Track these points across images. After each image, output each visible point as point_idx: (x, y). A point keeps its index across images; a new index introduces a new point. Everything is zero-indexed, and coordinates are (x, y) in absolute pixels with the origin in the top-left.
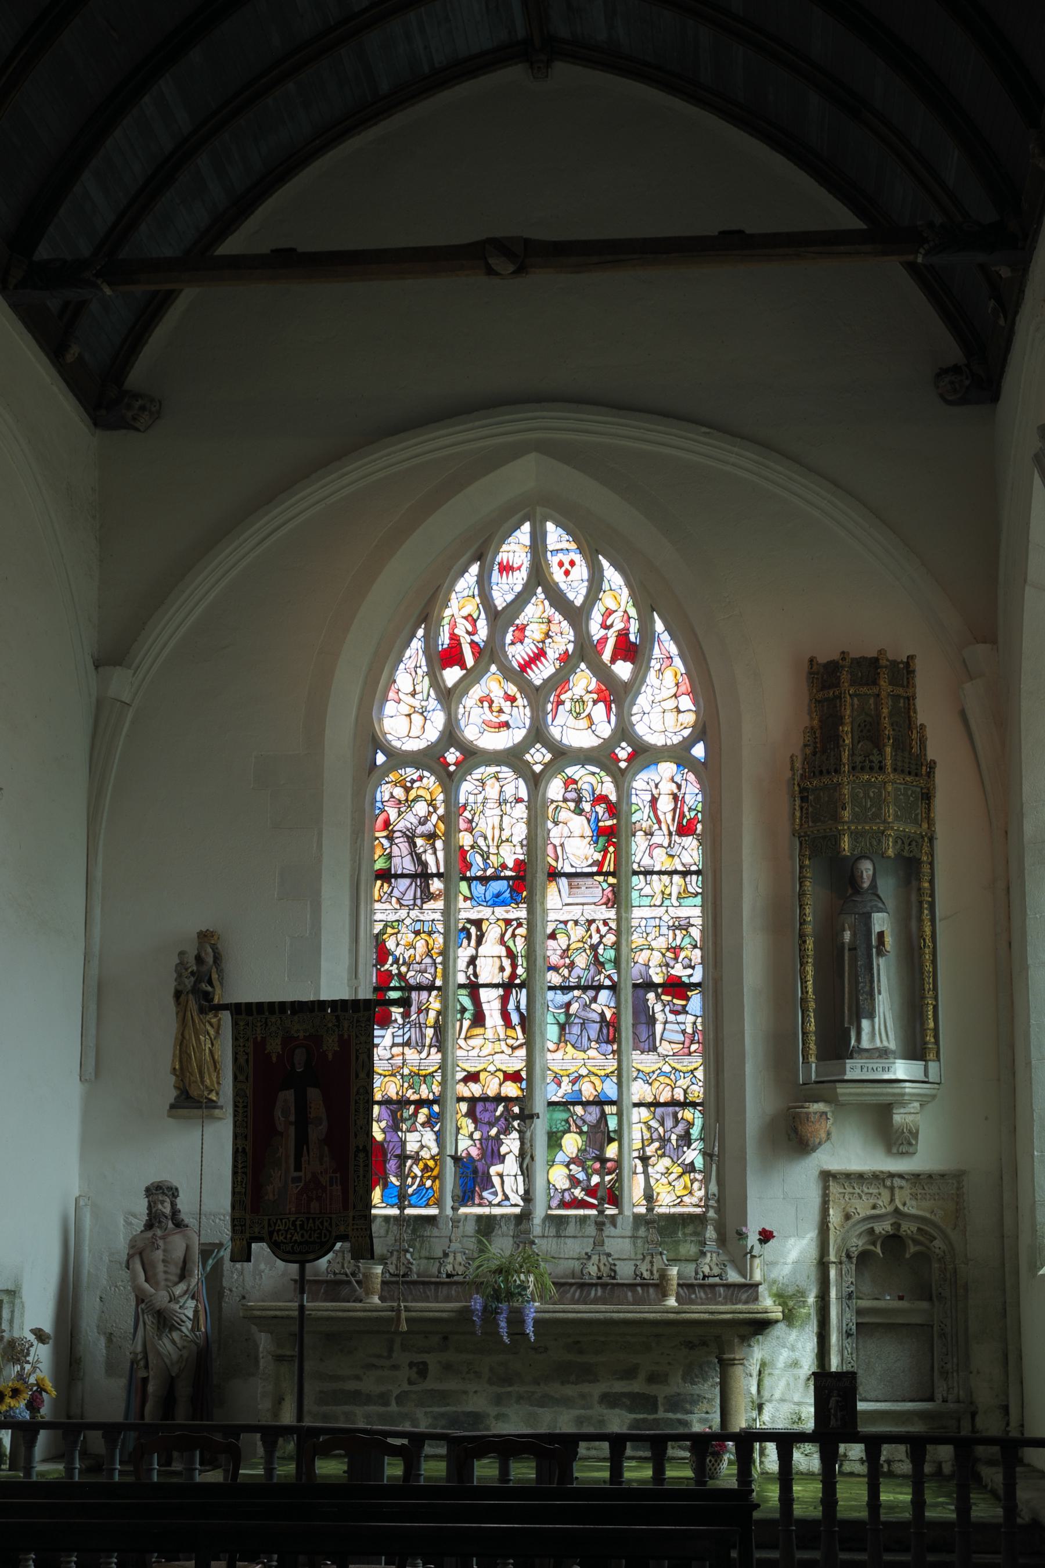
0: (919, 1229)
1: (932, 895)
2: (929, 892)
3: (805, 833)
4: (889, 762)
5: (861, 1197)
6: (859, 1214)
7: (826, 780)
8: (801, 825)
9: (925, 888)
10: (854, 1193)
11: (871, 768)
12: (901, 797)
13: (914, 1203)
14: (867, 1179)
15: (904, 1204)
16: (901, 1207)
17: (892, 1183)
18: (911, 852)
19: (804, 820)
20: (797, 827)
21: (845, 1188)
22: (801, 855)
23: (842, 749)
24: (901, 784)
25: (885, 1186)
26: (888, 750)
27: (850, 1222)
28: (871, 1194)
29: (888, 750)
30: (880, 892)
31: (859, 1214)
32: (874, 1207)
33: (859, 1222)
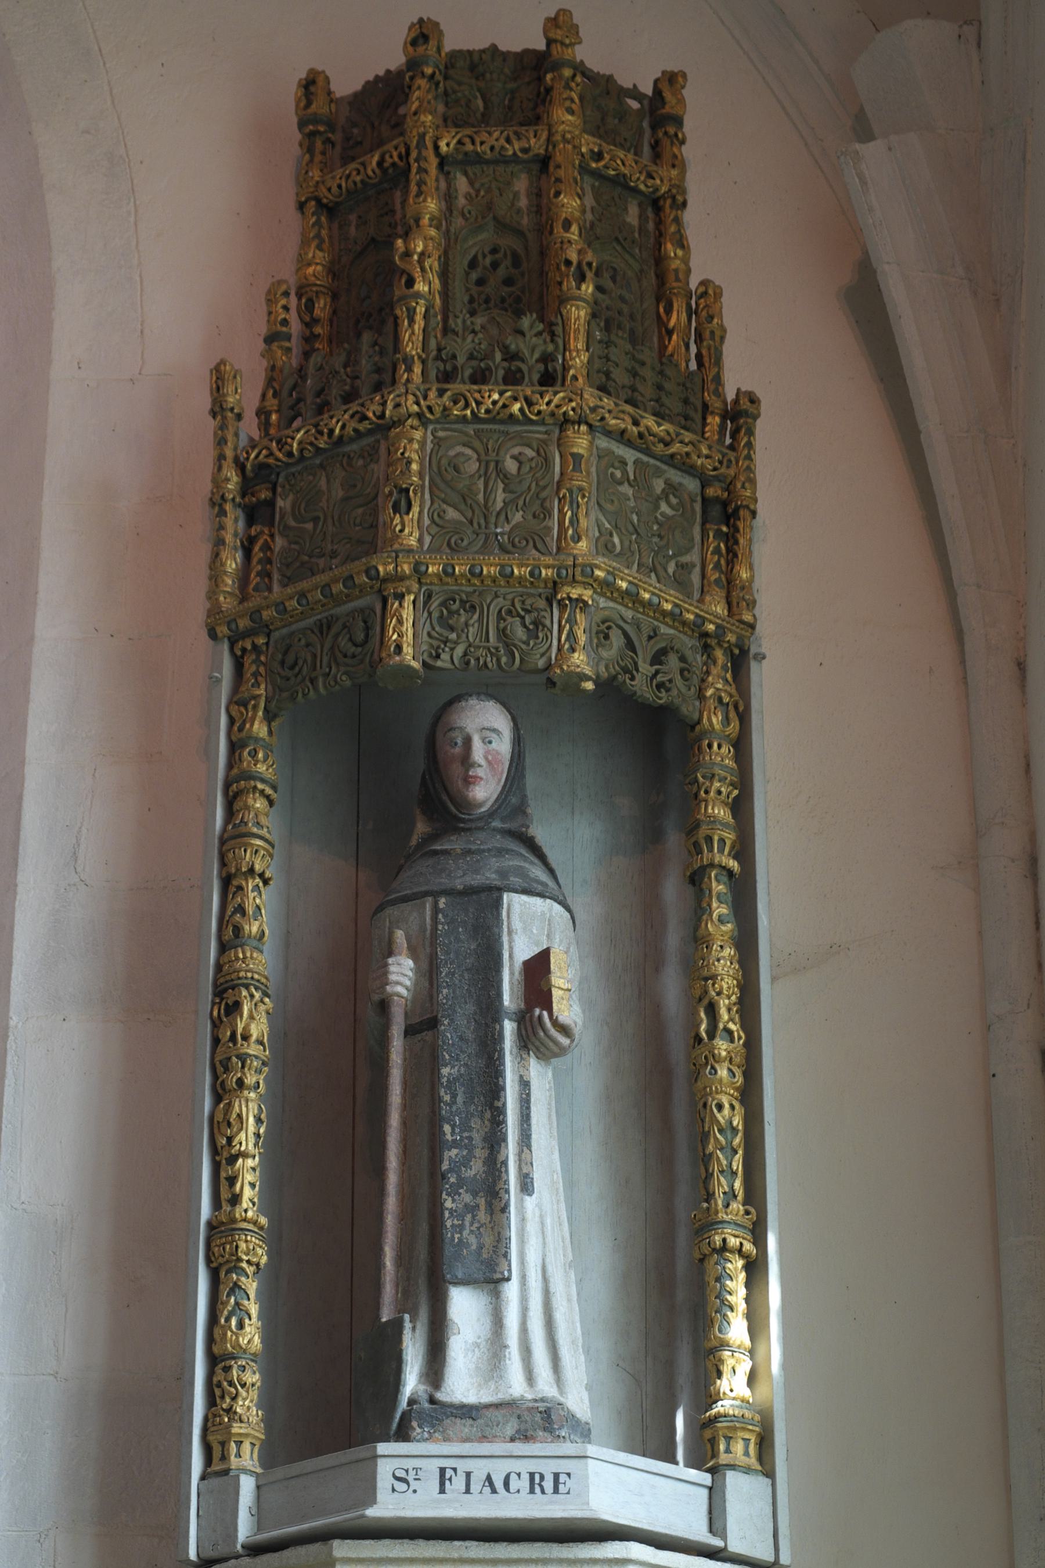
1: (744, 850)
2: (730, 836)
3: (255, 615)
4: (579, 360)
7: (339, 422)
8: (243, 599)
9: (713, 821)
11: (512, 378)
12: (626, 489)
18: (659, 686)
19: (254, 579)
20: (227, 603)
22: (239, 701)
23: (401, 312)
24: (621, 436)
26: (578, 314)
29: (578, 314)
30: (539, 832)
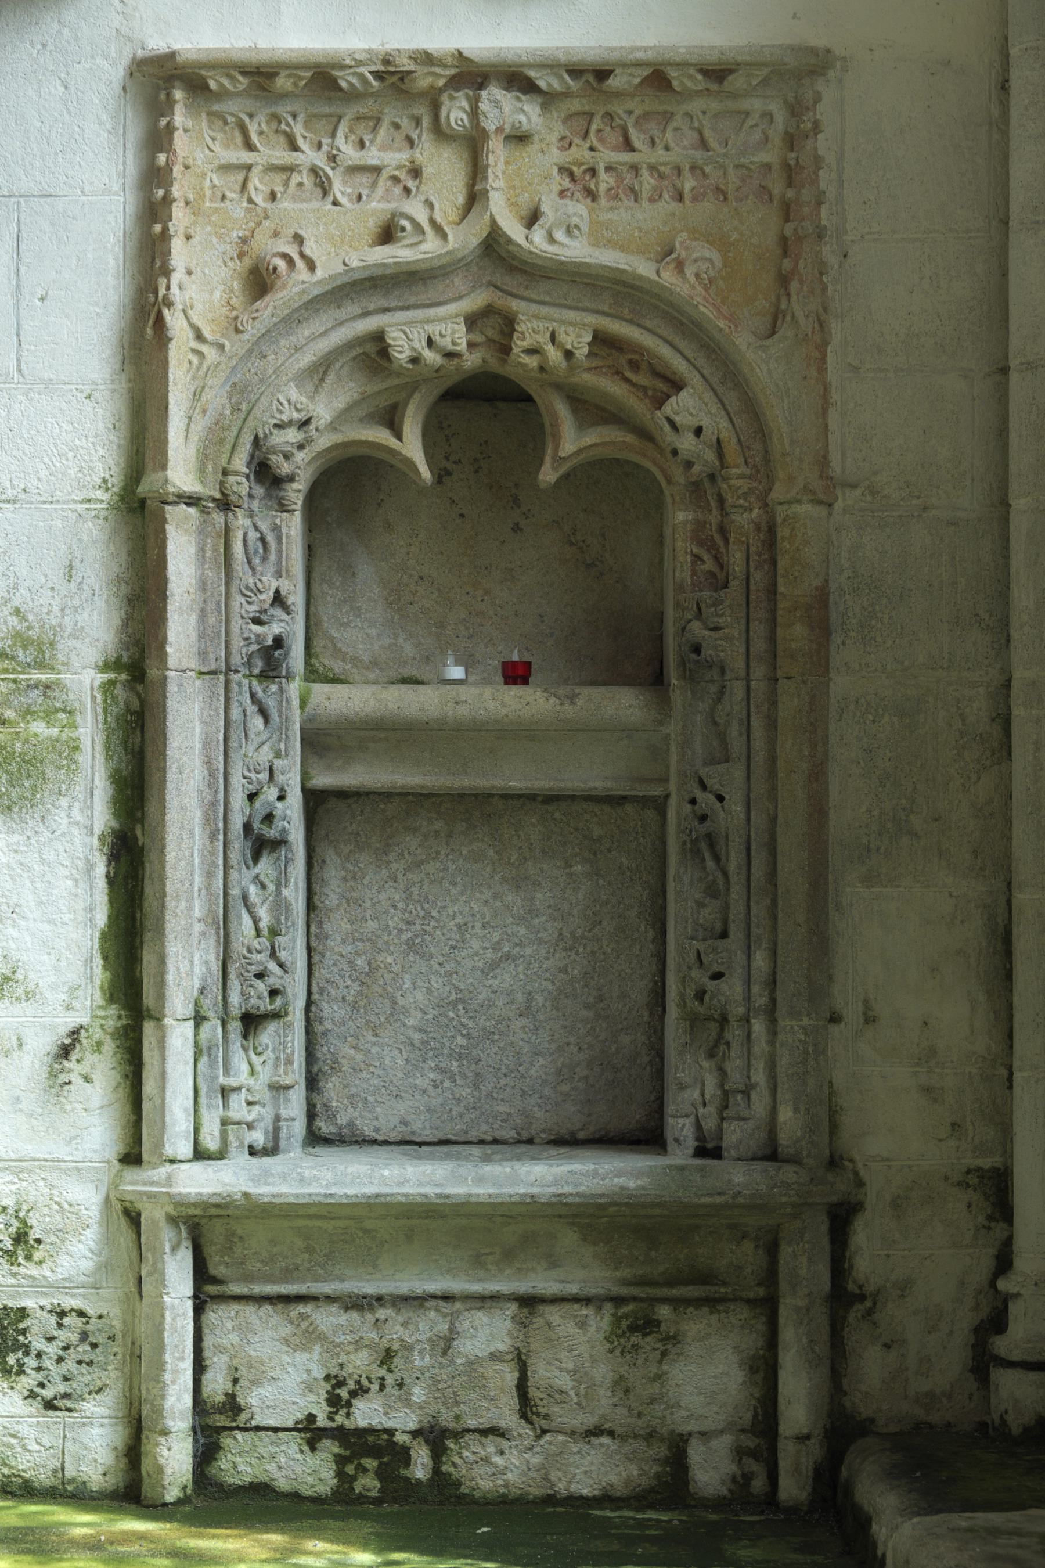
0: (602, 341)
5: (324, 187)
6: (311, 266)
10: (289, 169)
13: (578, 209)
14: (352, 96)
15: (532, 218)
16: (513, 229)
17: (474, 113)
21: (250, 146)
25: (440, 132)
27: (271, 307)
28: (377, 170)
31: (311, 266)
32: (387, 235)
33: (316, 304)
